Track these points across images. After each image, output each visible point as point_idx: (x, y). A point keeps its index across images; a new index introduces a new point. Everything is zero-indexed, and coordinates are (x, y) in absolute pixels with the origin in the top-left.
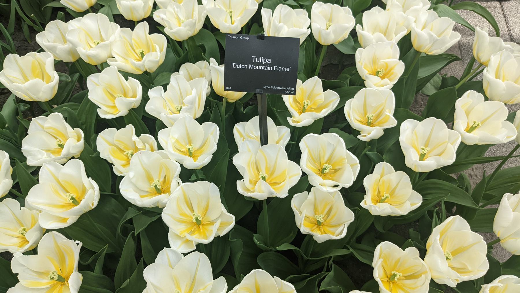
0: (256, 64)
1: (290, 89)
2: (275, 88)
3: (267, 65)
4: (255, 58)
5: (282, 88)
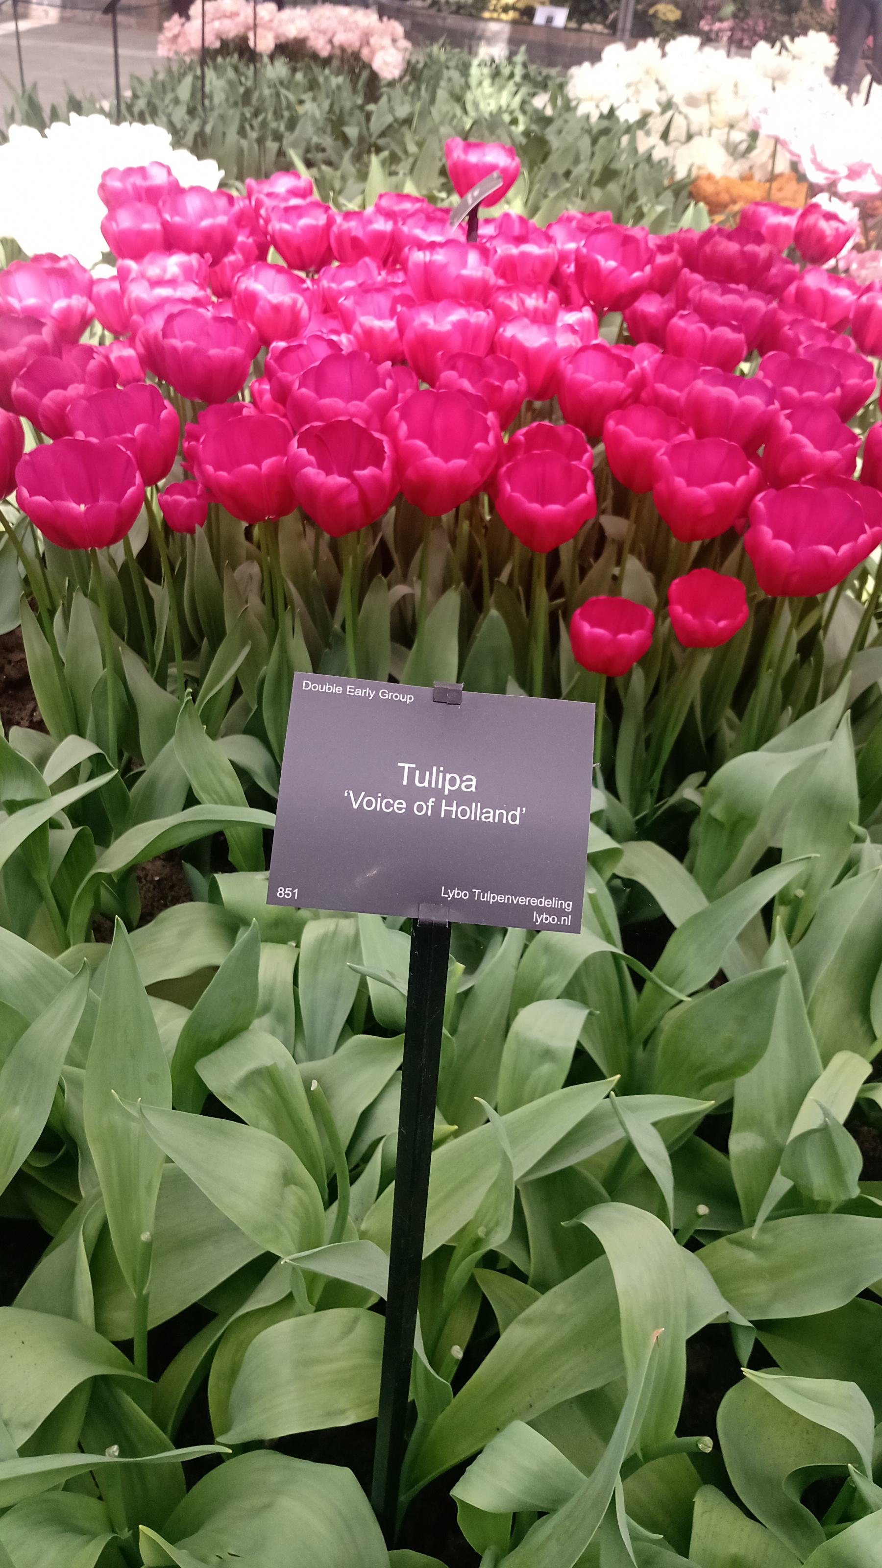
0: (412, 794)
1: (555, 903)
2: (489, 898)
4: (411, 772)
5: (522, 900)
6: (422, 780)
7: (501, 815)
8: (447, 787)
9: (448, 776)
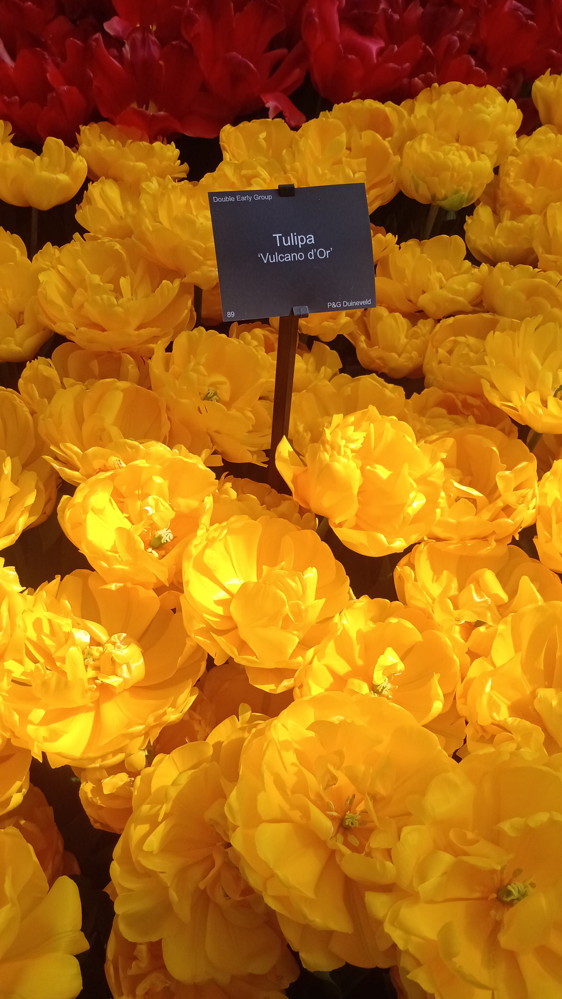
3: (306, 248)
6: (287, 242)
7: (294, 256)
8: (300, 243)
9: (299, 237)
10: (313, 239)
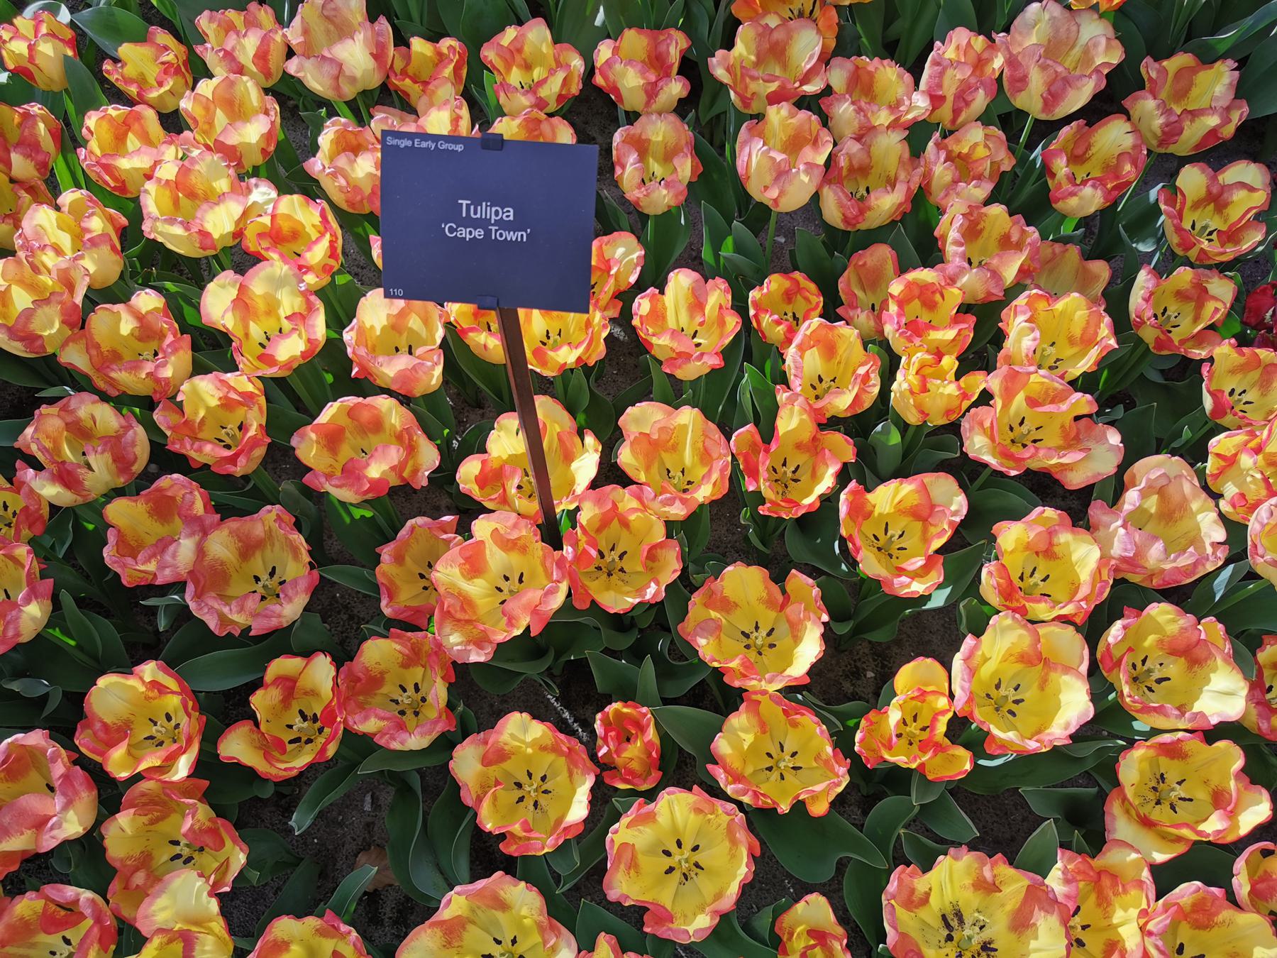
3: (502, 224)
6: (475, 213)
8: (493, 217)
10: (511, 214)
